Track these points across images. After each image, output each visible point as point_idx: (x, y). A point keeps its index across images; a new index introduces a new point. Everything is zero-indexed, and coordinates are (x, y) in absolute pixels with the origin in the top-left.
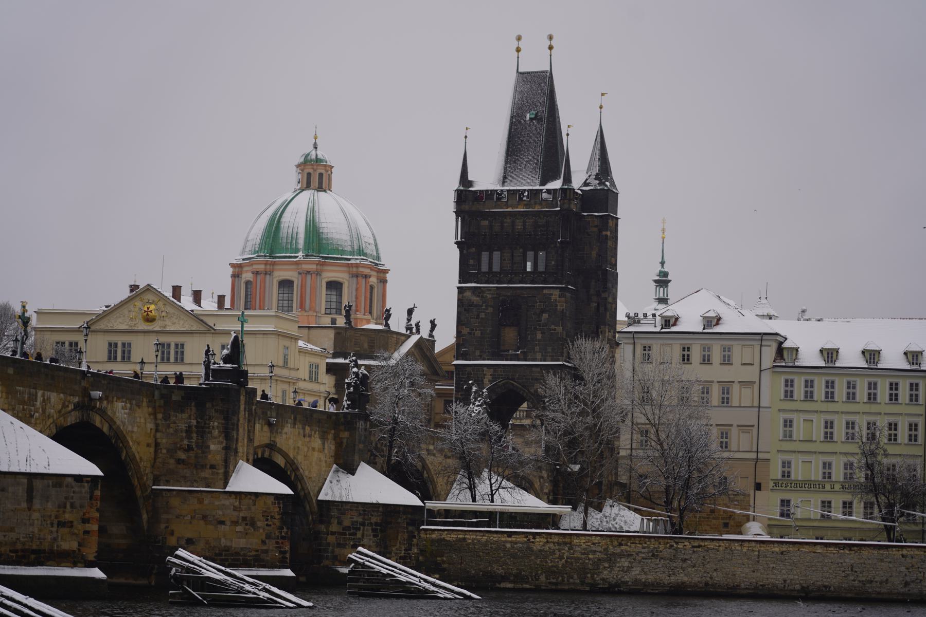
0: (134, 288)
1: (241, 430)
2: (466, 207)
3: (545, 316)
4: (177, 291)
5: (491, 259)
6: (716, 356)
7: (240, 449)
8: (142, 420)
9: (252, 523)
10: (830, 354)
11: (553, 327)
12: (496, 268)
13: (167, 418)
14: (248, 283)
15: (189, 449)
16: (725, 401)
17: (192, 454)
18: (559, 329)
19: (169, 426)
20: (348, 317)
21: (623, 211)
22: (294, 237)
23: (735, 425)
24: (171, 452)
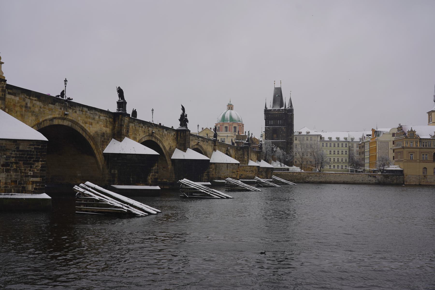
0: (203, 128)
4: (211, 128)
6: (309, 138)
9: (253, 171)
10: (330, 138)
12: (272, 124)
13: (237, 152)
14: (219, 127)
20: (238, 133)
21: (295, 113)
22: (227, 119)
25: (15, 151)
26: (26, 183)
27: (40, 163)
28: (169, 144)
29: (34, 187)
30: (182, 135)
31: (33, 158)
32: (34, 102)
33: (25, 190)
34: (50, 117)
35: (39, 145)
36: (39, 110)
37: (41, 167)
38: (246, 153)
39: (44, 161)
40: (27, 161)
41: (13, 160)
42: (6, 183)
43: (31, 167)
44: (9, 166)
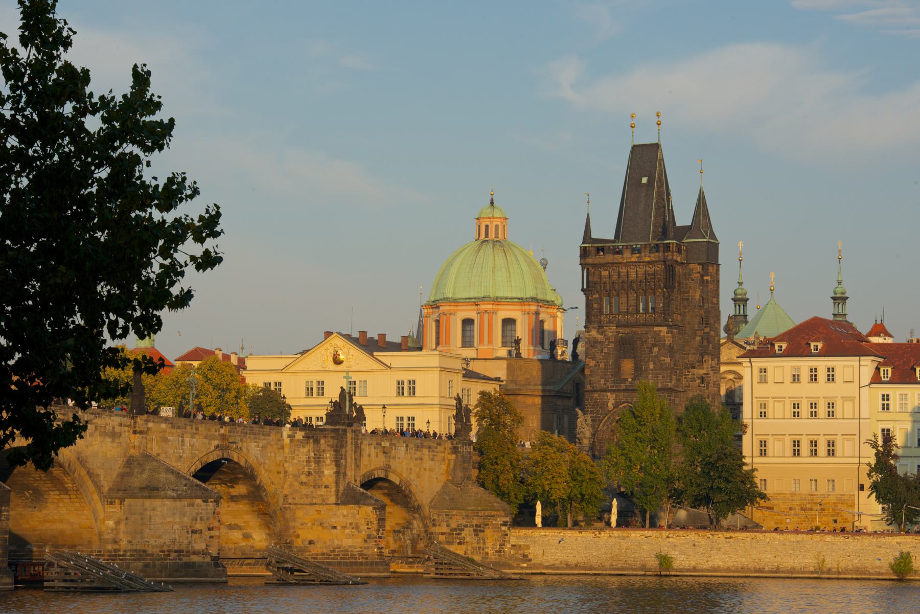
1: (349, 459)
2: (589, 260)
3: (656, 349)
5: (610, 303)
6: (822, 375)
7: (349, 473)
8: (273, 454)
9: (357, 528)
11: (663, 358)
15: (309, 473)
16: (831, 414)
17: (311, 478)
18: (668, 360)
19: (294, 458)
23: (839, 434)
24: (296, 477)
38: (329, 455)
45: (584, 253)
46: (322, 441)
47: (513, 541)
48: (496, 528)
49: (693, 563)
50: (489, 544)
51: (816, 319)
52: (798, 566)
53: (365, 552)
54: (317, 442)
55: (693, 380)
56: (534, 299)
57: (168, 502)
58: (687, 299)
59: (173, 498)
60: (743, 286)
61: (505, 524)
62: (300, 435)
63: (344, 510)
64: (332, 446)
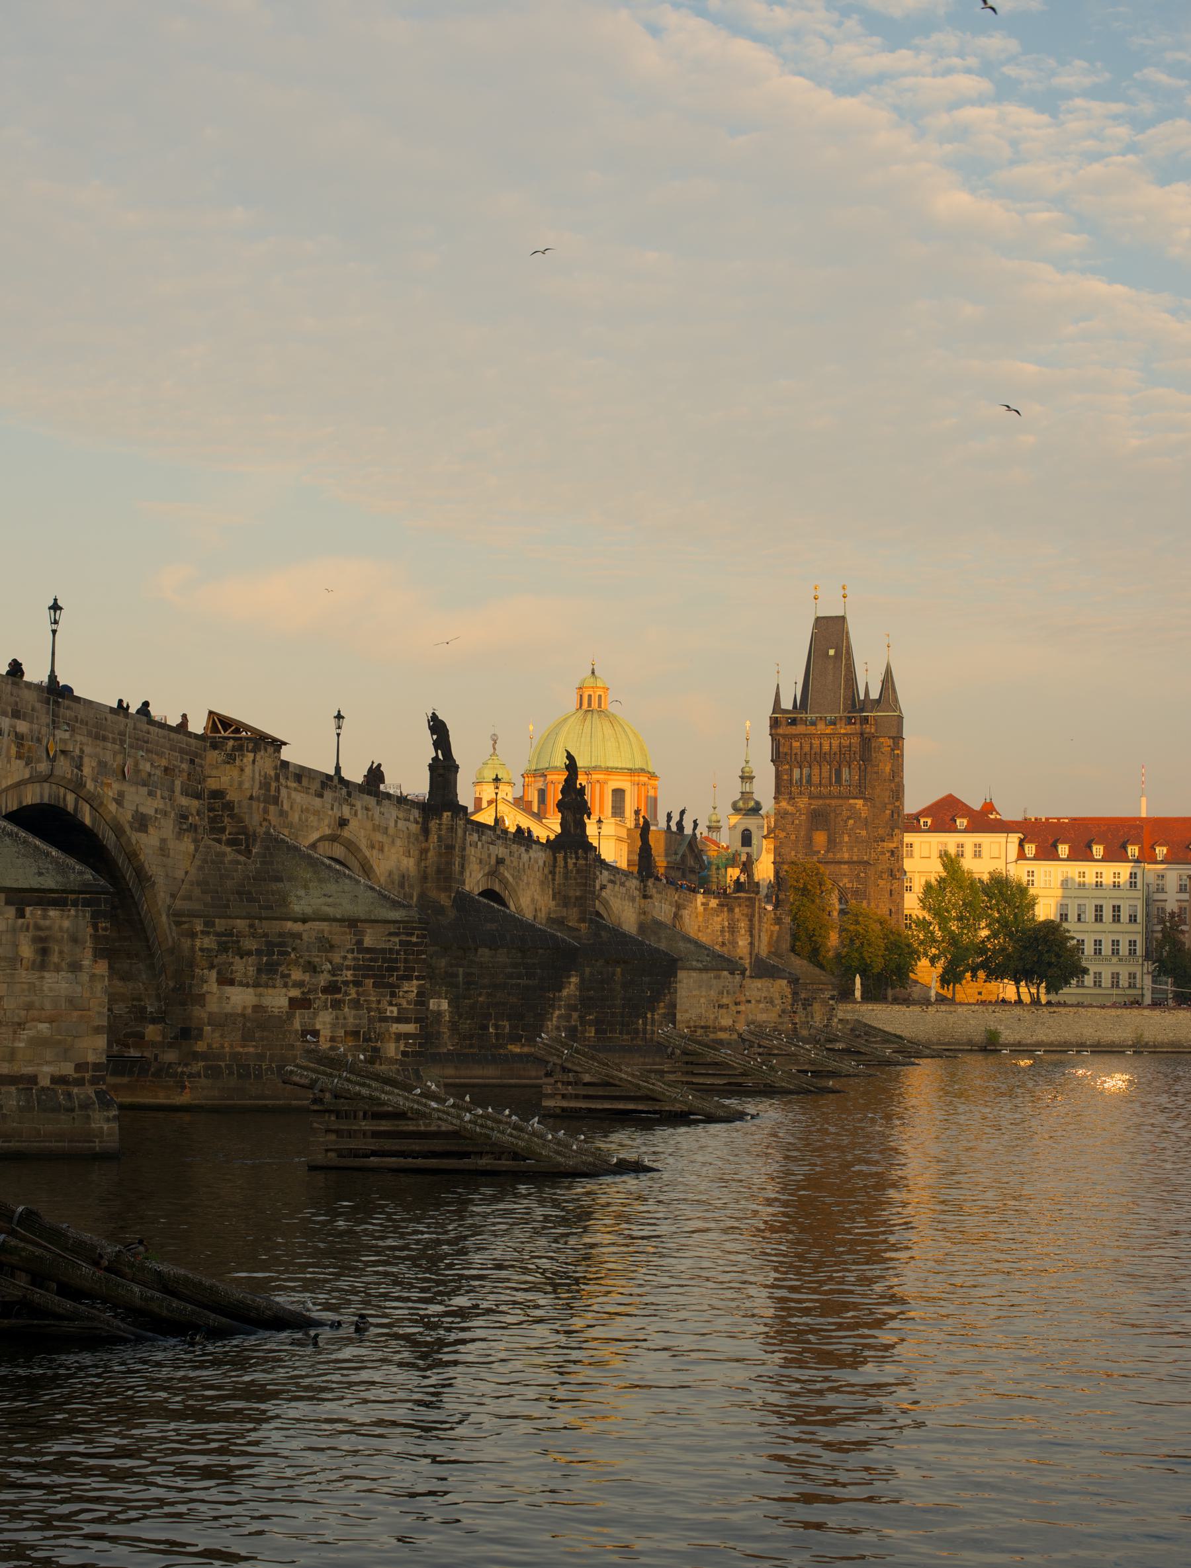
2: (780, 731)
3: (851, 822)
9: (772, 1002)
15: (723, 944)
17: (725, 949)
18: (864, 833)
25: (352, 951)
26: (380, 1037)
27: (415, 982)
28: (533, 900)
29: (402, 1048)
30: (570, 866)
31: (397, 969)
32: (294, 794)
33: (380, 1058)
34: (315, 836)
35: (412, 934)
36: (300, 819)
37: (417, 995)
38: (743, 925)
39: (423, 978)
40: (383, 977)
41: (348, 975)
42: (332, 1039)
43: (393, 995)
44: (338, 990)
45: (775, 723)
46: (737, 910)
47: (840, 1015)
48: (824, 1002)
49: (1018, 1038)
50: (817, 1017)
51: (950, 796)
52: (1116, 1040)
53: (780, 1027)
54: (731, 910)
55: (883, 853)
56: (642, 770)
57: (694, 974)
58: (877, 773)
59: (700, 969)
60: (750, 764)
61: (832, 998)
62: (714, 903)
63: (758, 983)
64: (747, 915)
